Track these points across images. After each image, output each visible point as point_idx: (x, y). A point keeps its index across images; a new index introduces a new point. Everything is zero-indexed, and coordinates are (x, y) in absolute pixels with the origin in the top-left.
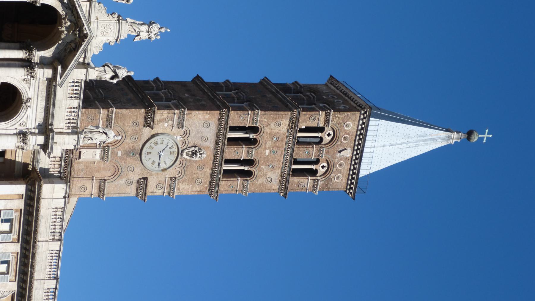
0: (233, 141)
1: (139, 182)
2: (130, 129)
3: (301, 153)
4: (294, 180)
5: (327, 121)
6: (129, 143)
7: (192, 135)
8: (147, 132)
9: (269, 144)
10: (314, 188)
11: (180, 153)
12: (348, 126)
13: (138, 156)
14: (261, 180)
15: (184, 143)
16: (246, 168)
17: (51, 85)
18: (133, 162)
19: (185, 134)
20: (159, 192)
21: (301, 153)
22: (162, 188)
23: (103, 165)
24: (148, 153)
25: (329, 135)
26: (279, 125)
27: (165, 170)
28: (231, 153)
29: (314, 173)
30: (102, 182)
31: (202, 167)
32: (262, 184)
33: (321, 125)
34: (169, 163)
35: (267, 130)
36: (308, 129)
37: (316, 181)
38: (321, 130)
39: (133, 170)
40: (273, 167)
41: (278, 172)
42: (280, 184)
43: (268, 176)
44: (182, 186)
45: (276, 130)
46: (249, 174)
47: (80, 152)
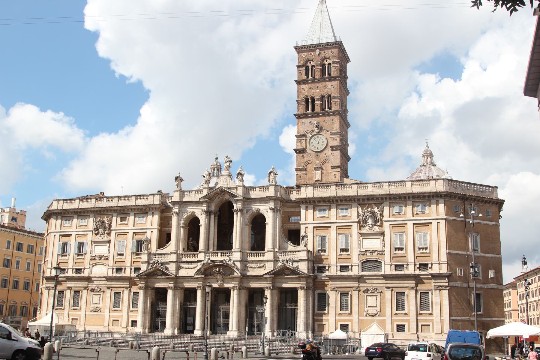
0: (313, 109)
1: (332, 150)
2: (306, 159)
4: (333, 74)
7: (308, 129)
12: (304, 55)
13: (319, 154)
20: (338, 139)
21: (318, 75)
22: (334, 139)
25: (310, 63)
26: (303, 89)
28: (318, 109)
30: (333, 167)
31: (325, 121)
33: (304, 68)
35: (306, 94)
37: (334, 63)
39: (325, 154)
40: (325, 86)
41: (328, 83)
42: (334, 80)
44: (335, 129)
45: (306, 89)
46: (329, 96)
47: (316, 181)
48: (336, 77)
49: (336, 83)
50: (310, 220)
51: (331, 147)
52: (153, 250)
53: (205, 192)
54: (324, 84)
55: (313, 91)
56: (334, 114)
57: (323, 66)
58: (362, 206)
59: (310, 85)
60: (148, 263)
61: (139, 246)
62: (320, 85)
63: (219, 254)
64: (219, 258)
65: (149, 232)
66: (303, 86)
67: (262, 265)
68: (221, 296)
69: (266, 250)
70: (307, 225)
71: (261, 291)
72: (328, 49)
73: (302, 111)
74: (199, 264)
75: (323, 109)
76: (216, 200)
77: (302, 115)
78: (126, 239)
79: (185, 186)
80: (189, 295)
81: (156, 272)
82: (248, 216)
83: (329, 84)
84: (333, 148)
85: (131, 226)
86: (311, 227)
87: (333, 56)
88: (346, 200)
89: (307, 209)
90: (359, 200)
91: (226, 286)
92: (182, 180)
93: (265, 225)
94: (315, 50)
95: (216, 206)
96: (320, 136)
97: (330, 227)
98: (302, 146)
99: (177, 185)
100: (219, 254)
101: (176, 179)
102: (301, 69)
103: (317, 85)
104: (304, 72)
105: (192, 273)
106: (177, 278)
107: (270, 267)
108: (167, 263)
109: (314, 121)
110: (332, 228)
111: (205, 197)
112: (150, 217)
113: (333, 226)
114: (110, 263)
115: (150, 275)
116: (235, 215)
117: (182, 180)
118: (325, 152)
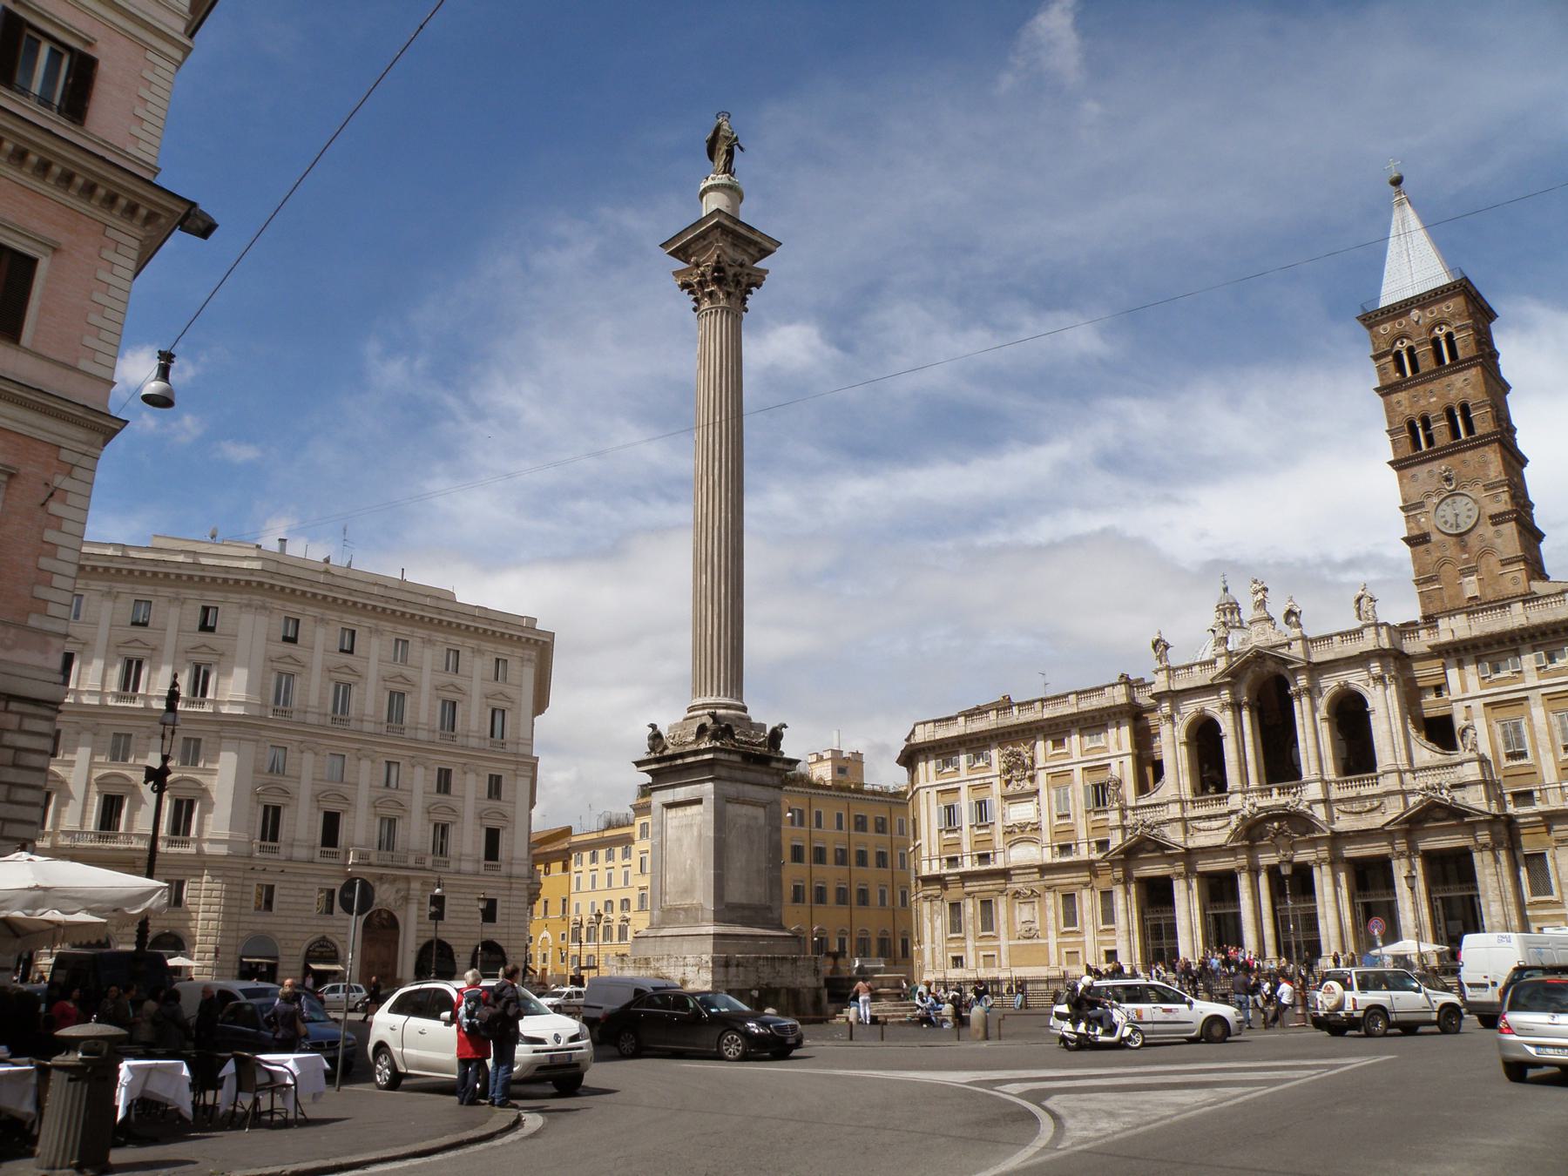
1: (1494, 524)
2: (1436, 555)
3: (1427, 364)
4: (1461, 355)
5: (1385, 354)
6: (1451, 550)
8: (1435, 537)
9: (1423, 402)
10: (1466, 327)
11: (1453, 494)
14: (1469, 390)
15: (1439, 494)
16: (1458, 413)
17: (1317, 669)
18: (1472, 540)
19: (1429, 496)
20: (1505, 497)
21: (1427, 364)
22: (1496, 496)
23: (1483, 569)
24: (1458, 526)
27: (1475, 501)
28: (1442, 437)
29: (1449, 336)
30: (1506, 562)
31: (1464, 462)
32: (1474, 388)
34: (1466, 500)
35: (1408, 412)
36: (1400, 368)
37: (1459, 329)
38: (1398, 357)
41: (1453, 377)
43: (1465, 385)
45: (1405, 403)
47: (1471, 599)
48: (1471, 359)
49: (1474, 373)
50: (1474, 687)
51: (1491, 517)
52: (1131, 802)
53: (1222, 664)
54: (1445, 381)
55: (1423, 402)
56: (1484, 441)
57: (1436, 342)
58: (1002, 746)
59: (1412, 391)
60: (1124, 828)
61: (1101, 794)
62: (1436, 386)
63: (1275, 791)
64: (1276, 799)
65: (1114, 763)
66: (1395, 397)
67: (1376, 803)
68: (1294, 885)
69: (1379, 770)
70: (1467, 703)
71: (1230, 878)
72: (1437, 302)
73: (1407, 451)
74: (1234, 817)
75: (1455, 433)
76: (1249, 676)
77: (1407, 459)
78: (1072, 782)
79: (1174, 659)
80: (1219, 890)
81: (1144, 846)
82: (1323, 703)
83: (1458, 380)
84: (1497, 519)
85: (1077, 757)
86: (1477, 705)
87: (1453, 316)
88: (1555, 632)
89: (1460, 665)
90: (1532, 637)
91: (1298, 858)
92: (1167, 647)
93: (1221, 739)
94: (1409, 312)
95: (1250, 690)
96: (1458, 498)
97: (1526, 698)
98: (1420, 528)
99: (1160, 658)
100: (1275, 791)
101: (1155, 646)
102: (1383, 361)
103: (1430, 387)
104: (1391, 367)
105: (1221, 838)
106: (1190, 855)
107: (1394, 809)
108: (1163, 823)
109: (1440, 466)
110: (1531, 701)
111: (1223, 674)
112: (1112, 732)
113: (1535, 696)
114: (1046, 837)
115: (1130, 854)
116: (1296, 704)
117: (1167, 647)
118: (1480, 530)
